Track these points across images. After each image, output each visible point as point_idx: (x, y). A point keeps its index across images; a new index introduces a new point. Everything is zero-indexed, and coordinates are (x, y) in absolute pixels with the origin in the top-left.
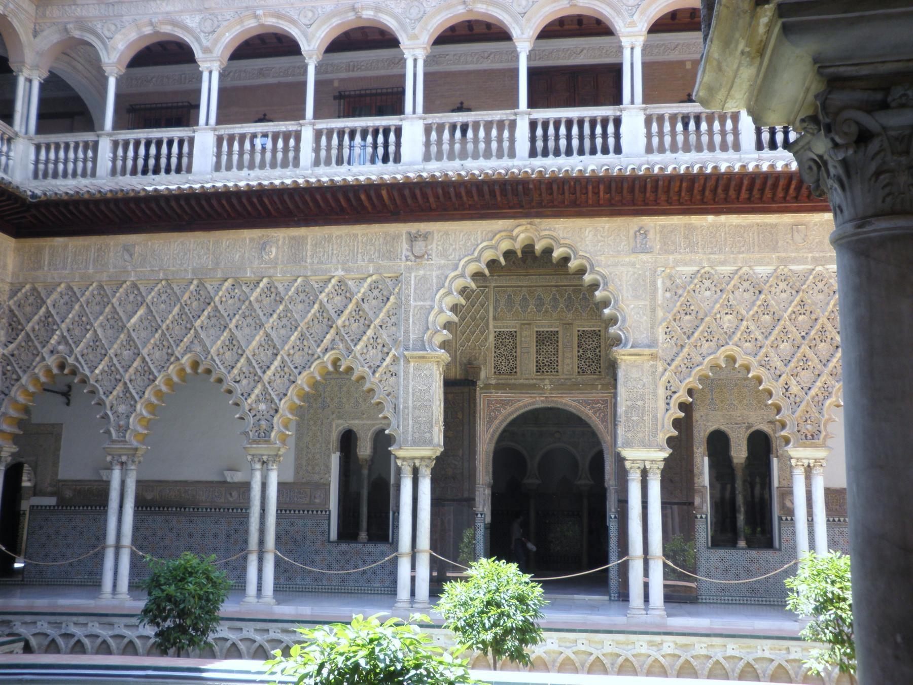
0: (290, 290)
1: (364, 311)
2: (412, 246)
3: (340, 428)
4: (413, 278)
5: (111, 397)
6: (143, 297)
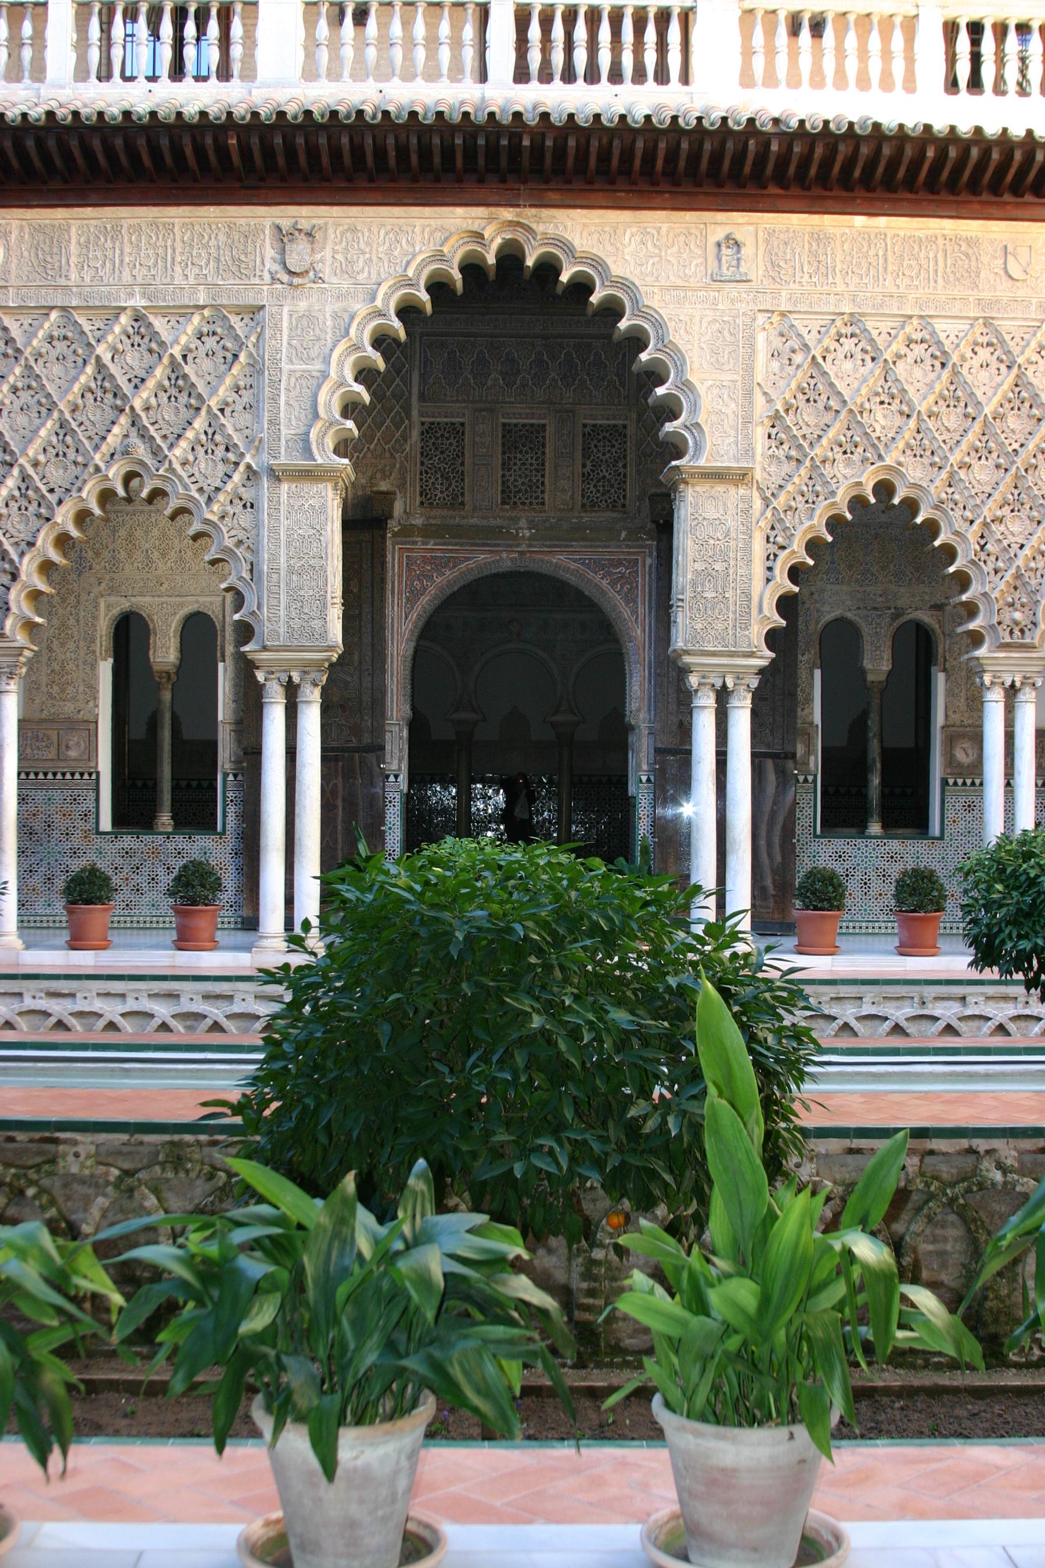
0: (35, 335)
1: (185, 377)
2: (283, 252)
3: (116, 612)
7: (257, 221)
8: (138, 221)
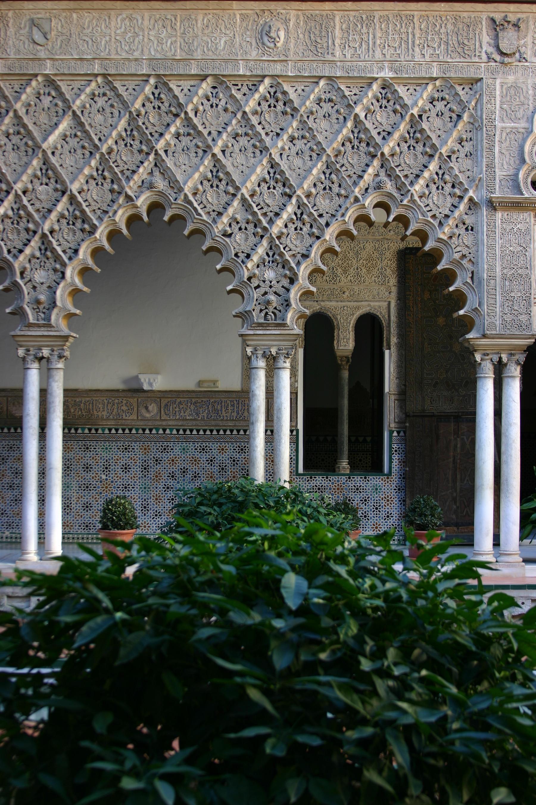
0: (308, 98)
1: (422, 131)
4: (498, 87)
5: (21, 257)
6: (65, 101)
7: (476, 14)
8: (387, 13)
